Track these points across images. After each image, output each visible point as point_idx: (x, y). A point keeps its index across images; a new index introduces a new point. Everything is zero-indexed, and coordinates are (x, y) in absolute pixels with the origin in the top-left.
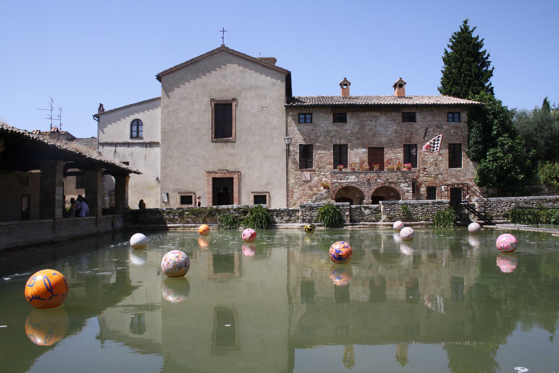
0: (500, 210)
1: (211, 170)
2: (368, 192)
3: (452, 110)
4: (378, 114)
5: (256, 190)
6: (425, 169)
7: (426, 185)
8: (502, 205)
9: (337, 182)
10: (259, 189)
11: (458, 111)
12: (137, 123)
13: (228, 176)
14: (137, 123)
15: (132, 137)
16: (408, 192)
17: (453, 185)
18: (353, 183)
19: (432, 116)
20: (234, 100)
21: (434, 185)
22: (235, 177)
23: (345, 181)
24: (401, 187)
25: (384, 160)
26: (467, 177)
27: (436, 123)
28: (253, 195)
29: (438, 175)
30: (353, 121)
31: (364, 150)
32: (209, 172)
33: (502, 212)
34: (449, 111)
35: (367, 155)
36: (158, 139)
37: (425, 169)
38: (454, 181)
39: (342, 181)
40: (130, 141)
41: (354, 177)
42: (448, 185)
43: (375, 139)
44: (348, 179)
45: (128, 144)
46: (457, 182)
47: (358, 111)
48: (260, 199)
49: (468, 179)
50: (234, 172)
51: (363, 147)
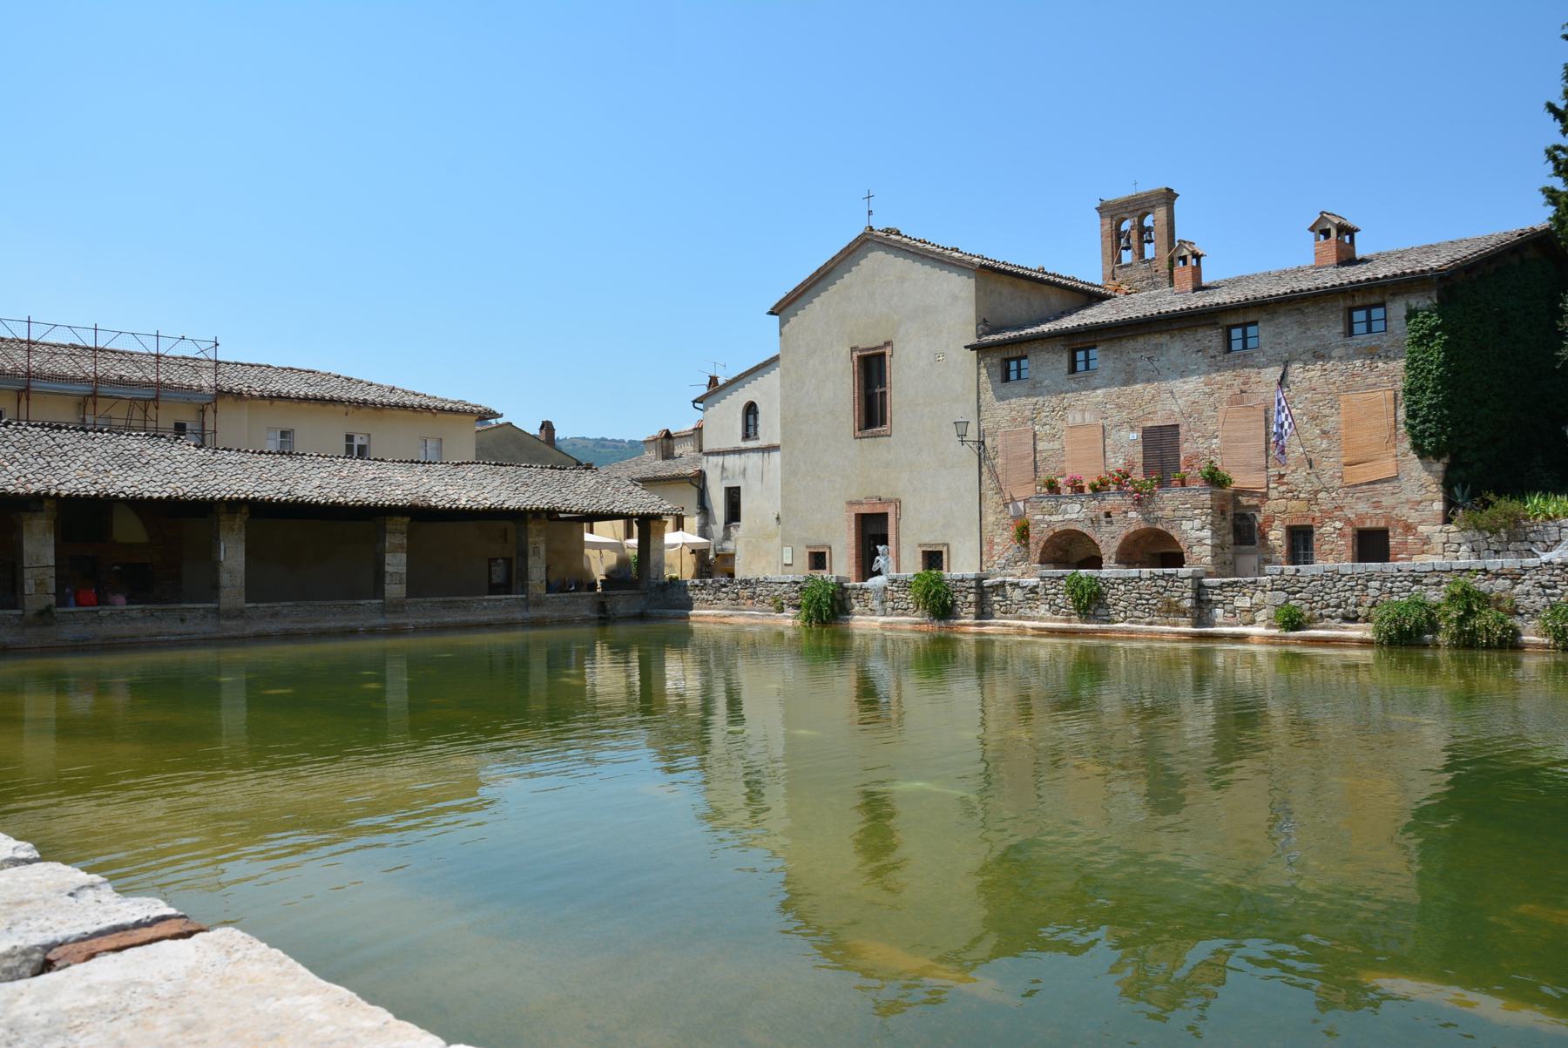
0: (1333, 602)
1: (854, 499)
2: (1108, 541)
3: (1359, 301)
4: (1164, 339)
5: (926, 540)
6: (1281, 476)
7: (1283, 521)
8: (1339, 585)
9: (1042, 521)
10: (932, 539)
11: (1375, 299)
12: (751, 409)
13: (879, 509)
14: (751, 409)
15: (746, 437)
16: (1200, 541)
17: (1361, 518)
18: (1076, 520)
19: (1301, 324)
20: (888, 344)
21: (1308, 522)
22: (891, 511)
23: (1060, 518)
24: (1185, 532)
25: (1178, 456)
26: (1403, 497)
27: (1312, 344)
28: (920, 550)
29: (1317, 492)
30: (1110, 364)
31: (1134, 436)
32: (850, 503)
33: (1338, 606)
34: (1349, 303)
35: (1140, 448)
36: (777, 442)
37: (1281, 476)
38: (1363, 507)
39: (1054, 518)
40: (743, 445)
41: (1077, 507)
42: (1348, 521)
43: (1159, 406)
44: (1065, 512)
45: (739, 451)
46: (1371, 511)
47: (1120, 339)
48: (933, 559)
49: (1407, 501)
50: (889, 501)
51: (1132, 429)
